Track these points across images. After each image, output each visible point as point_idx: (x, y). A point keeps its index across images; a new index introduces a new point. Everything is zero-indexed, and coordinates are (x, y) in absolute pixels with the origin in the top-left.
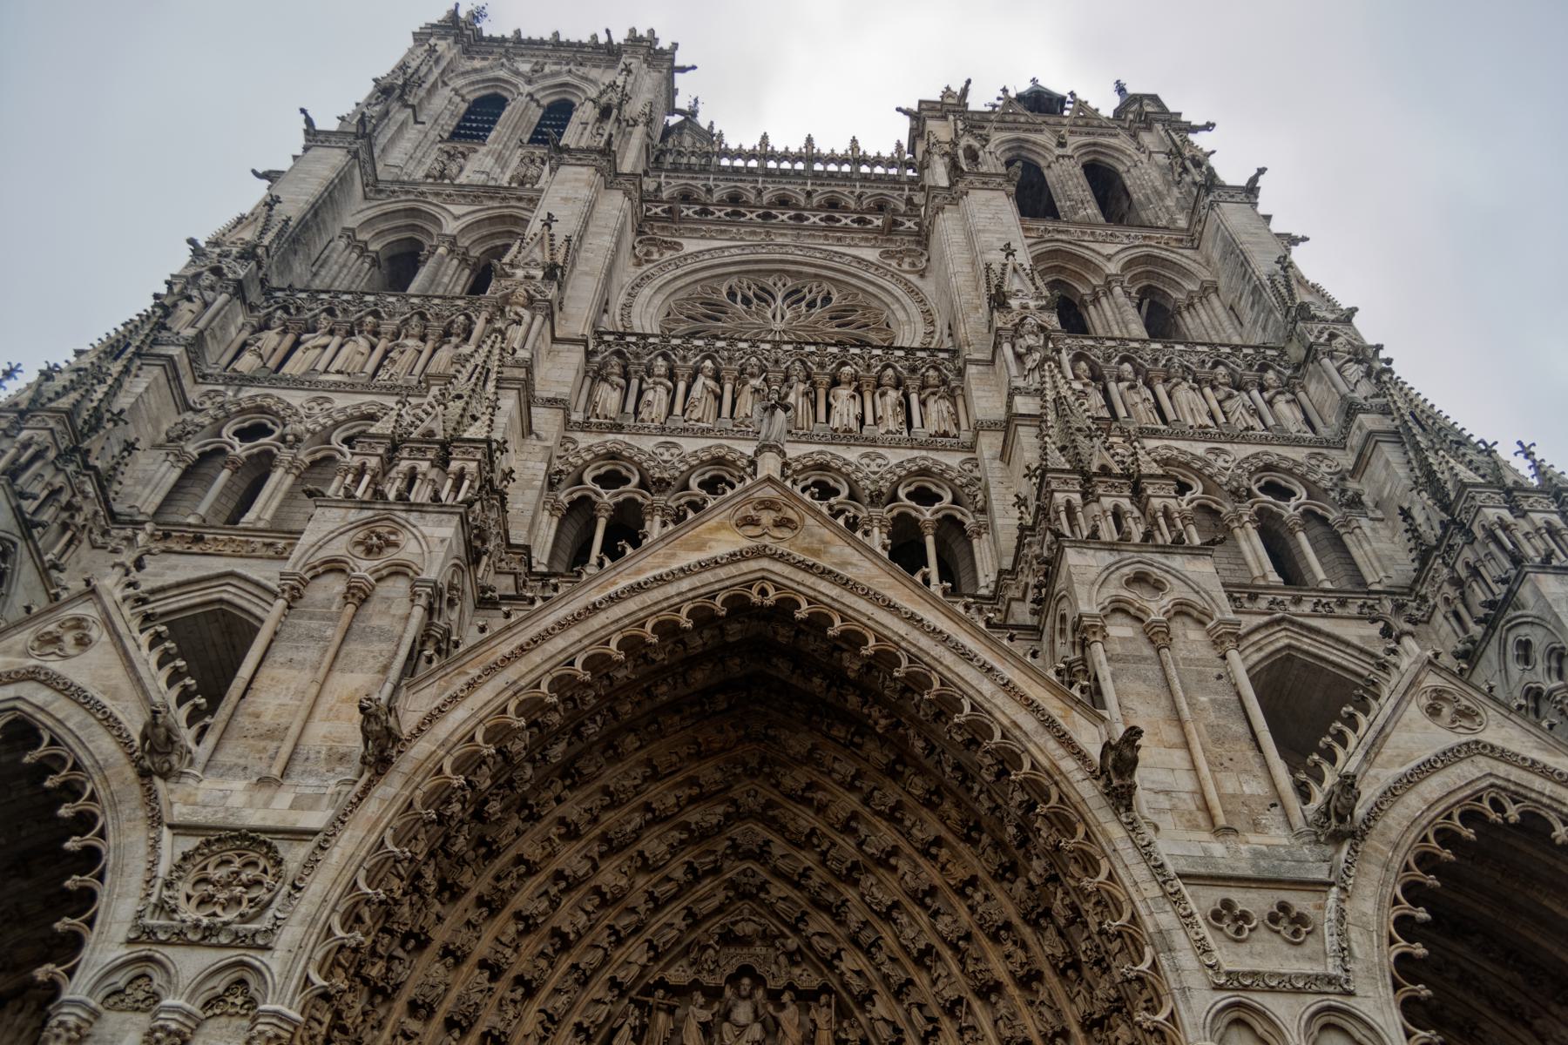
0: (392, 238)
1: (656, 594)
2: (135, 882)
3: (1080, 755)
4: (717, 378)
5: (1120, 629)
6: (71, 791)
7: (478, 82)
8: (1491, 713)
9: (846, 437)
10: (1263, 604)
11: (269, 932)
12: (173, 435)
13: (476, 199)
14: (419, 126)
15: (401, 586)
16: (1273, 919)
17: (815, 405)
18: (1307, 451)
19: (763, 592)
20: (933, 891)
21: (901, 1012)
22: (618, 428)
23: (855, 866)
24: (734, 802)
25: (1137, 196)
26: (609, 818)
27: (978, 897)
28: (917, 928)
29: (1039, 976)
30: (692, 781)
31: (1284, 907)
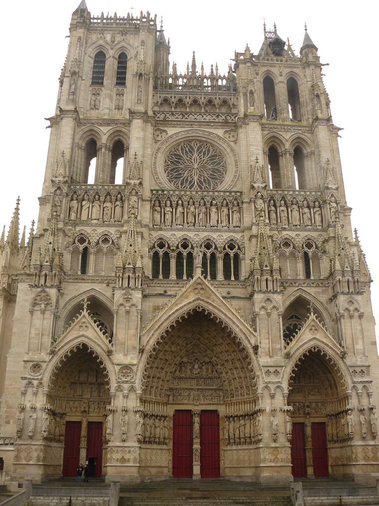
0: (87, 139)
1: (180, 311)
2: (113, 373)
3: (251, 344)
4: (182, 205)
5: (263, 312)
6: (97, 357)
7: (95, 48)
8: (320, 330)
9: (214, 228)
10: (297, 284)
11: (135, 381)
13: (109, 125)
14: (83, 81)
15: (134, 309)
16: (274, 372)
17: (207, 215)
18: (319, 233)
19: (199, 308)
20: (228, 351)
21: (222, 368)
22: (161, 229)
23: (215, 344)
24: (194, 332)
25: (301, 100)
26: (173, 339)
27: (235, 353)
28: (225, 356)
29: (244, 368)
30: (186, 330)
31: (276, 370)
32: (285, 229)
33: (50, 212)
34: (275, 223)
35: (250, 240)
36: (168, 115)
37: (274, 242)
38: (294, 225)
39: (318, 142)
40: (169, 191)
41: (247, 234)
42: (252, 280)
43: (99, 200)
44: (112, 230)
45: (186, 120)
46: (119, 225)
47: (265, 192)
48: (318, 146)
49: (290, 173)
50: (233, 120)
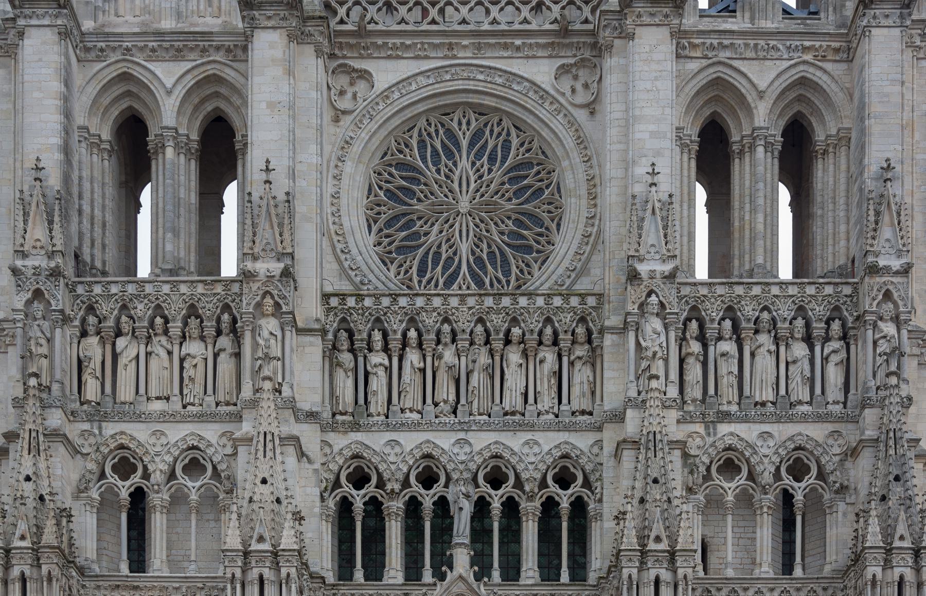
12: (82, 488)
18: (830, 427)
32: (726, 417)
33: (19, 376)
34: (700, 397)
35: (617, 455)
36: (372, 9)
37: (691, 461)
38: (756, 404)
39: (862, 96)
40: (377, 297)
41: (610, 436)
42: (615, 582)
43: (166, 332)
44: (211, 433)
45: (434, 27)
46: (230, 414)
47: (674, 292)
48: (861, 115)
49: (760, 218)
50: (586, 21)
